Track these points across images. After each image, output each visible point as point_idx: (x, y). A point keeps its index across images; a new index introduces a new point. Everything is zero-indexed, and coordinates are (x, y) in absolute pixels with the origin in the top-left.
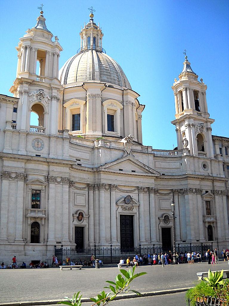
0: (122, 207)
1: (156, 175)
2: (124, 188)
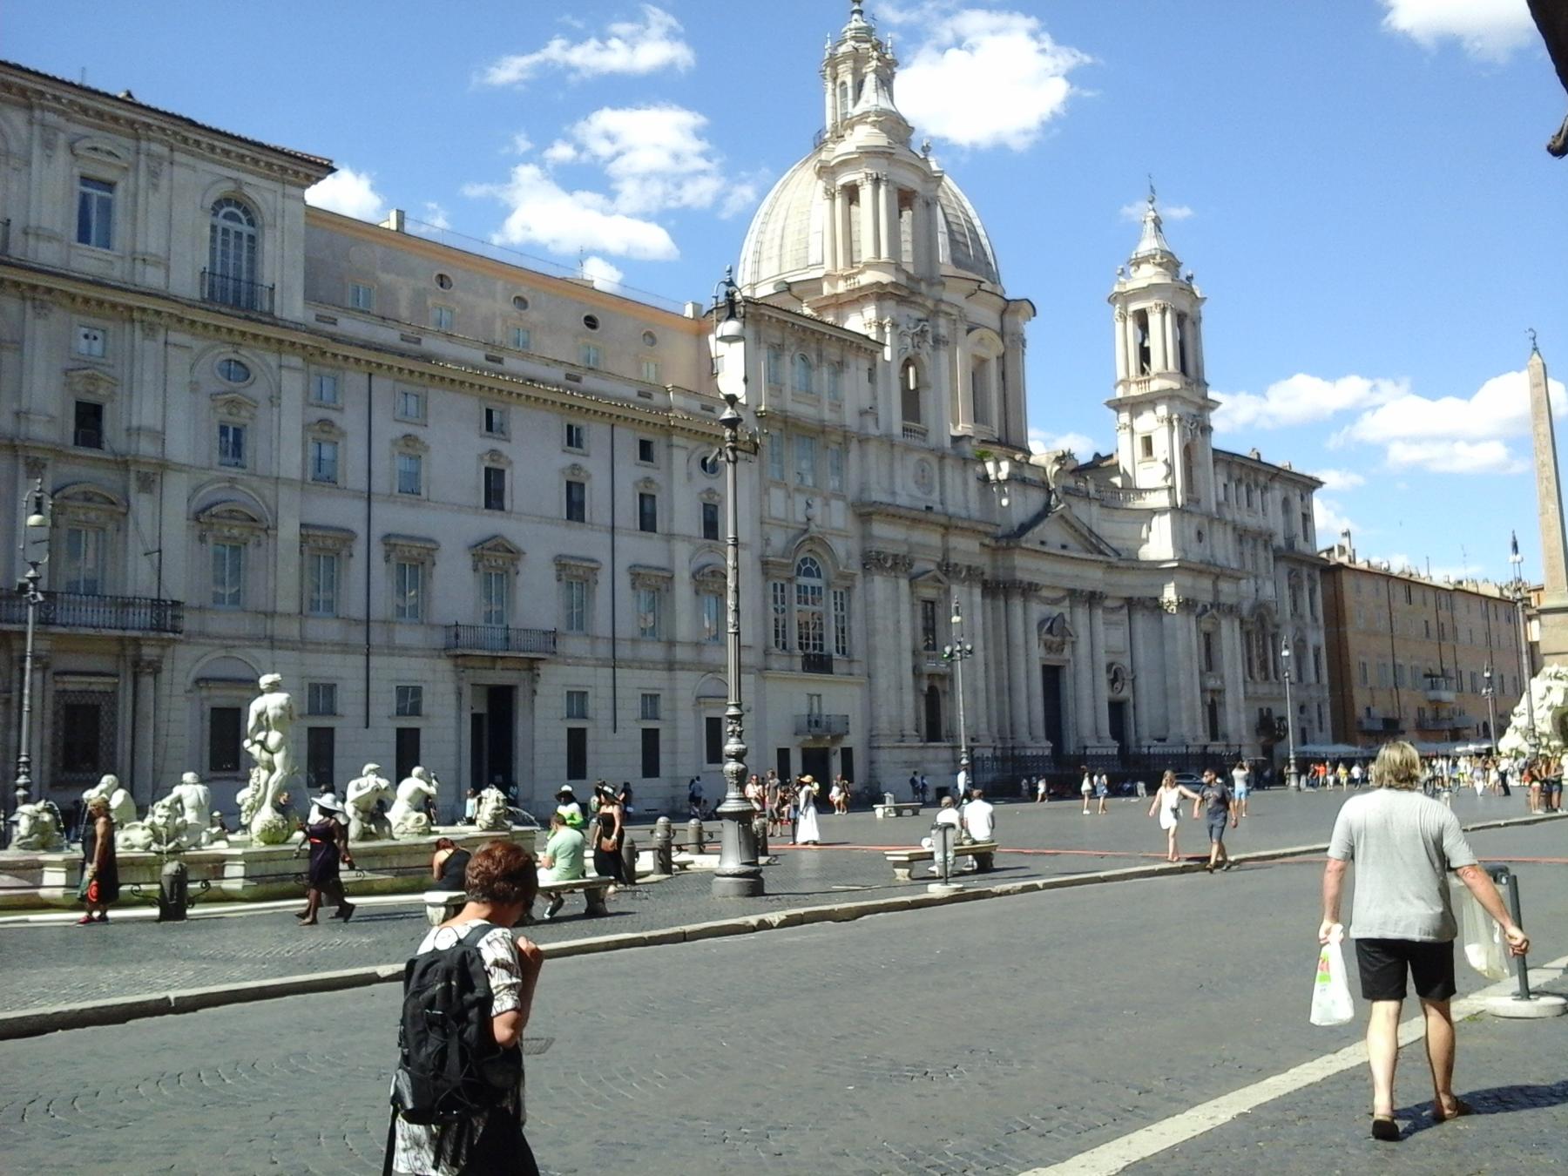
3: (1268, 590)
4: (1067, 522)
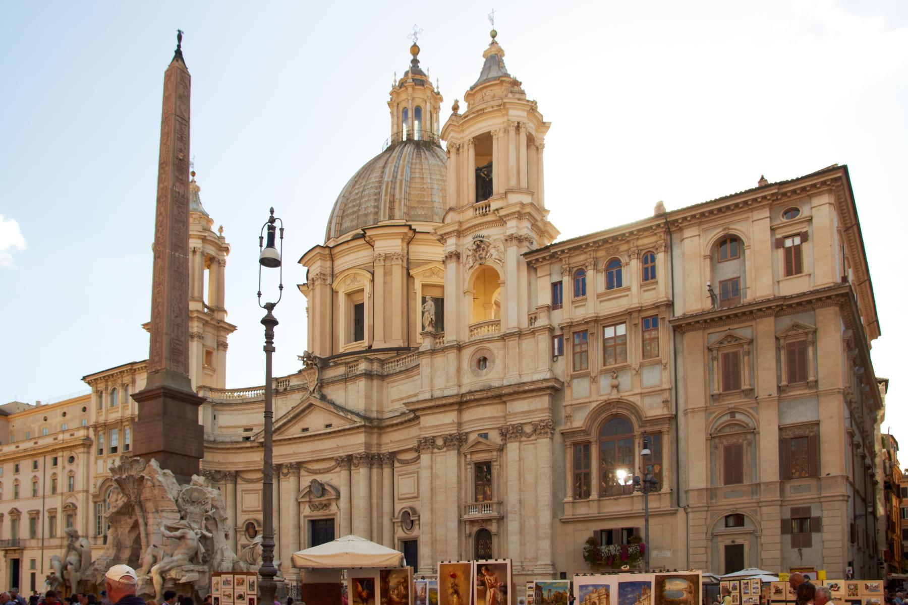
1: (358, 424)
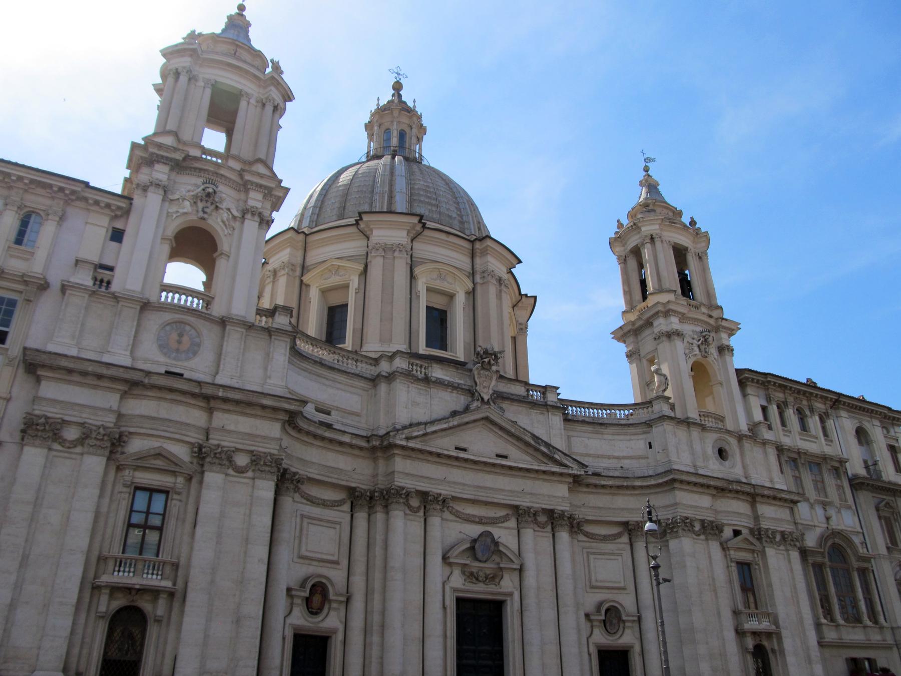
0: (463, 573)
1: (575, 472)
2: (470, 510)
3: (846, 521)
4: (502, 428)
